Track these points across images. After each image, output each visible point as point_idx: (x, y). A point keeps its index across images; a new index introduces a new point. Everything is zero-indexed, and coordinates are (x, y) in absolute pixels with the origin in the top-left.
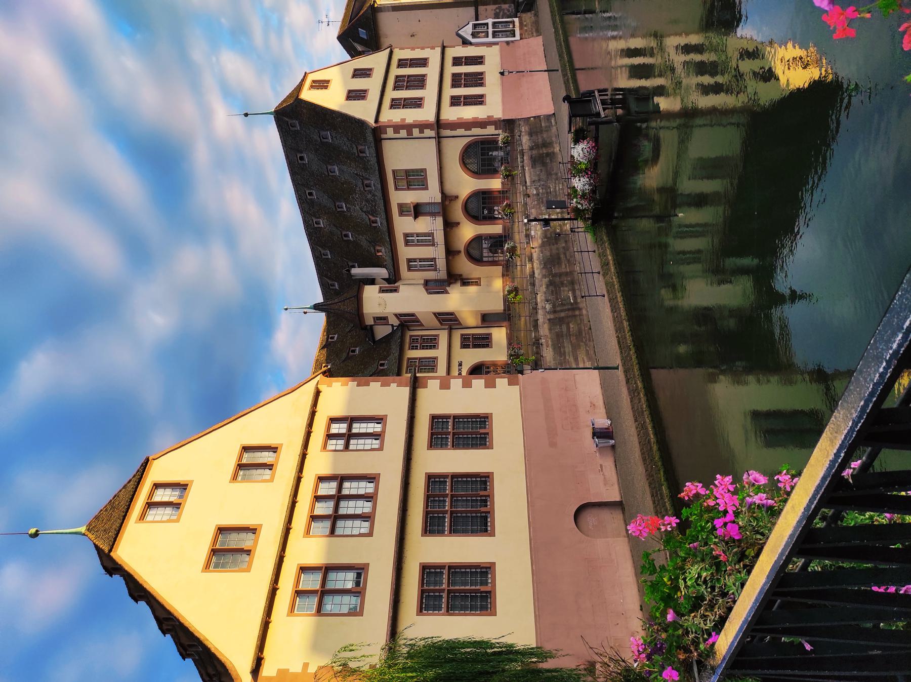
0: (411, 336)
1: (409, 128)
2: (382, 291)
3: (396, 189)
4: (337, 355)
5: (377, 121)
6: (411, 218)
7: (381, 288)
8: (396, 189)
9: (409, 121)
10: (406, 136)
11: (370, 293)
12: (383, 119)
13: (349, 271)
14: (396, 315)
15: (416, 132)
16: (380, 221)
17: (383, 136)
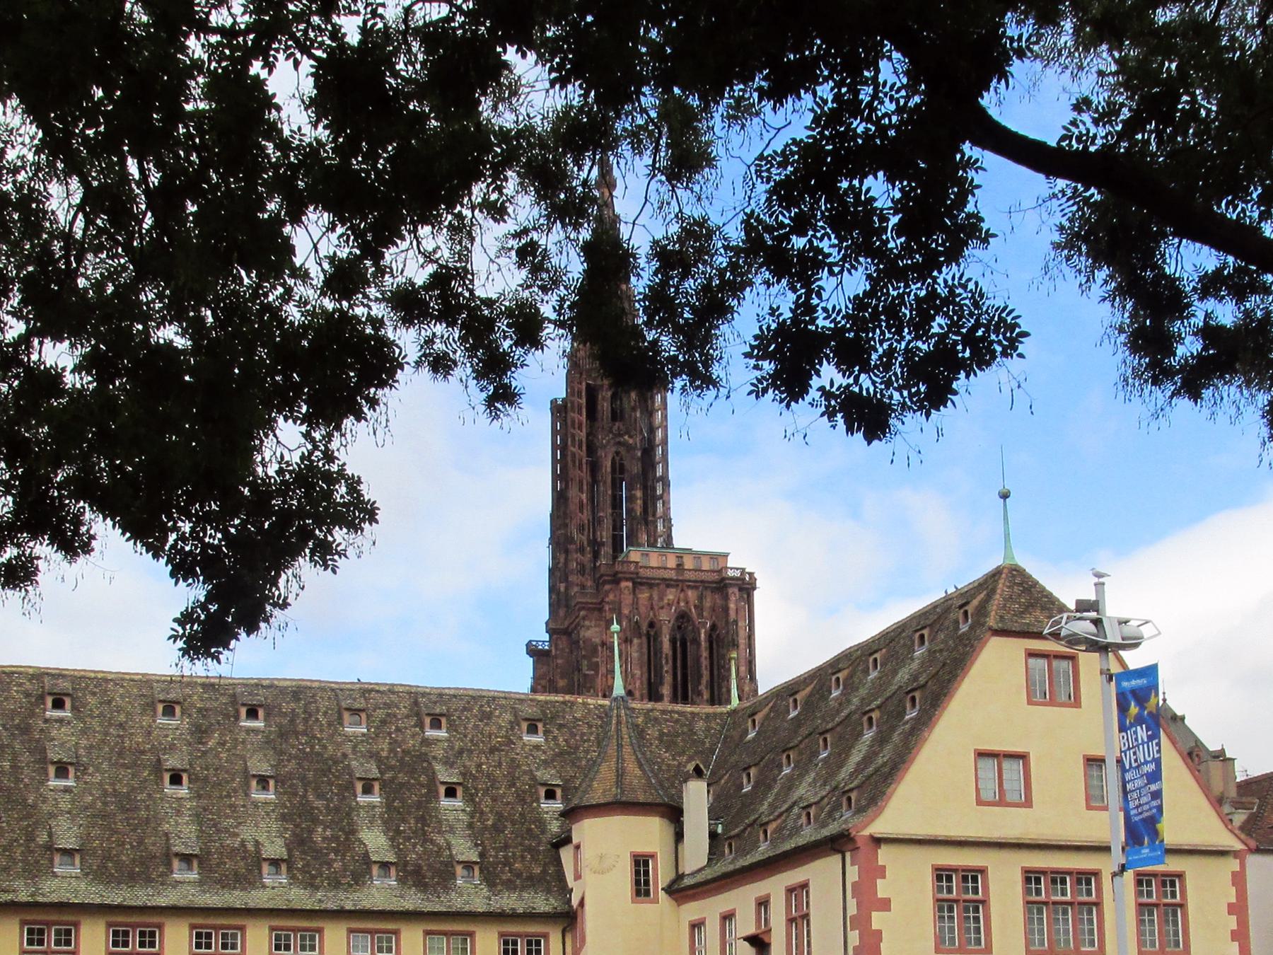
0: (546, 936)
1: (861, 922)
2: (641, 864)
3: (790, 890)
4: (561, 754)
5: (878, 841)
6: (751, 930)
7: (653, 856)
8: (790, 890)
9: (878, 920)
10: (849, 914)
11: (649, 833)
12: (885, 855)
13: (698, 773)
14: (582, 903)
15: (854, 938)
16: (763, 850)
17: (848, 855)
